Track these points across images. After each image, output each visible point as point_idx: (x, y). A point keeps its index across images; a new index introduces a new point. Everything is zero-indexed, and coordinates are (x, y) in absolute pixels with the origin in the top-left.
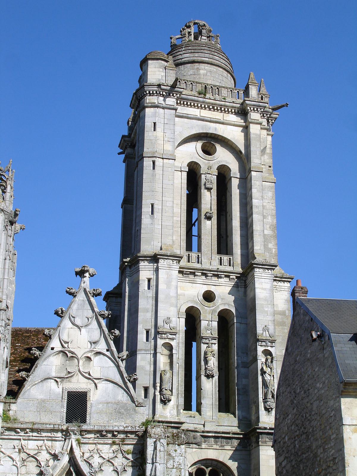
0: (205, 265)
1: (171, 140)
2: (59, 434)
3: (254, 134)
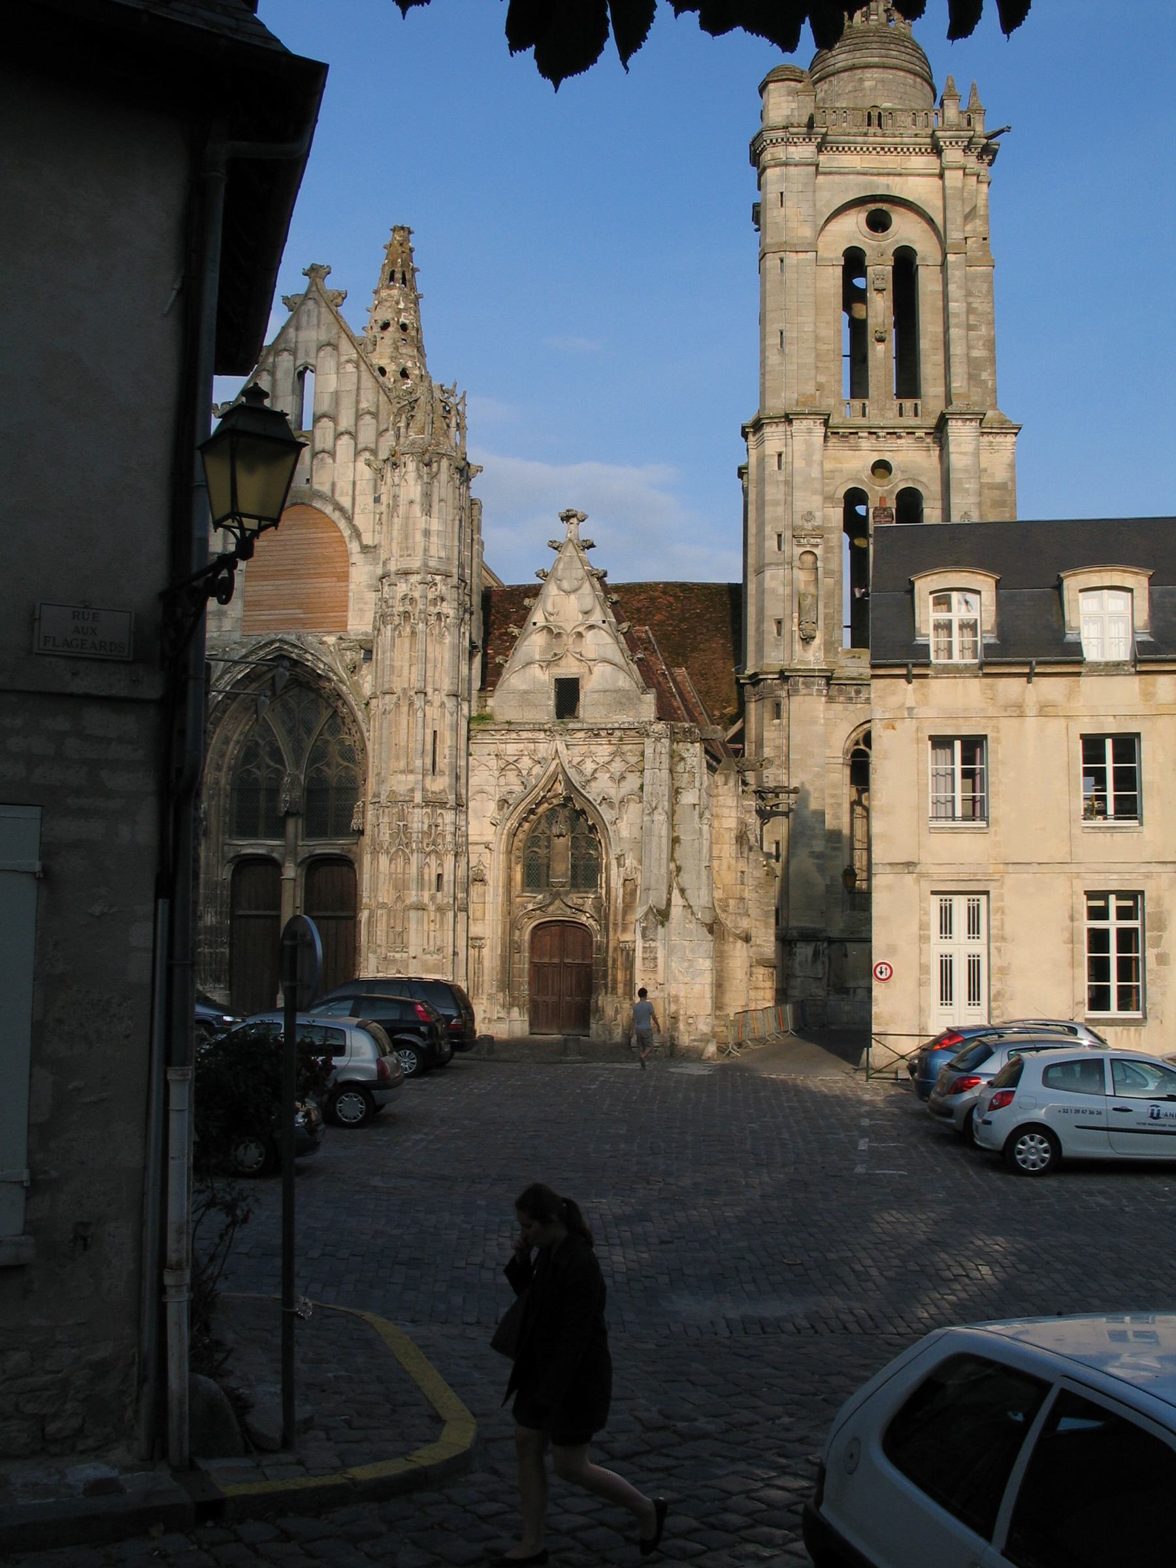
0: (875, 417)
1: (810, 218)
2: (542, 735)
3: (951, 188)
